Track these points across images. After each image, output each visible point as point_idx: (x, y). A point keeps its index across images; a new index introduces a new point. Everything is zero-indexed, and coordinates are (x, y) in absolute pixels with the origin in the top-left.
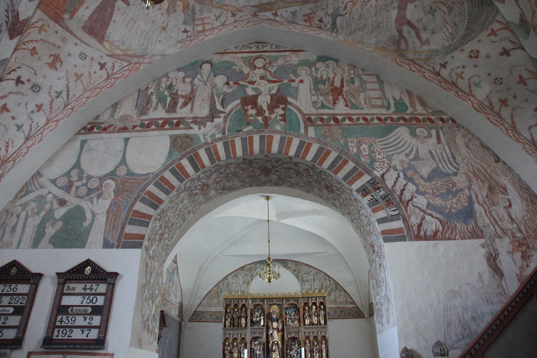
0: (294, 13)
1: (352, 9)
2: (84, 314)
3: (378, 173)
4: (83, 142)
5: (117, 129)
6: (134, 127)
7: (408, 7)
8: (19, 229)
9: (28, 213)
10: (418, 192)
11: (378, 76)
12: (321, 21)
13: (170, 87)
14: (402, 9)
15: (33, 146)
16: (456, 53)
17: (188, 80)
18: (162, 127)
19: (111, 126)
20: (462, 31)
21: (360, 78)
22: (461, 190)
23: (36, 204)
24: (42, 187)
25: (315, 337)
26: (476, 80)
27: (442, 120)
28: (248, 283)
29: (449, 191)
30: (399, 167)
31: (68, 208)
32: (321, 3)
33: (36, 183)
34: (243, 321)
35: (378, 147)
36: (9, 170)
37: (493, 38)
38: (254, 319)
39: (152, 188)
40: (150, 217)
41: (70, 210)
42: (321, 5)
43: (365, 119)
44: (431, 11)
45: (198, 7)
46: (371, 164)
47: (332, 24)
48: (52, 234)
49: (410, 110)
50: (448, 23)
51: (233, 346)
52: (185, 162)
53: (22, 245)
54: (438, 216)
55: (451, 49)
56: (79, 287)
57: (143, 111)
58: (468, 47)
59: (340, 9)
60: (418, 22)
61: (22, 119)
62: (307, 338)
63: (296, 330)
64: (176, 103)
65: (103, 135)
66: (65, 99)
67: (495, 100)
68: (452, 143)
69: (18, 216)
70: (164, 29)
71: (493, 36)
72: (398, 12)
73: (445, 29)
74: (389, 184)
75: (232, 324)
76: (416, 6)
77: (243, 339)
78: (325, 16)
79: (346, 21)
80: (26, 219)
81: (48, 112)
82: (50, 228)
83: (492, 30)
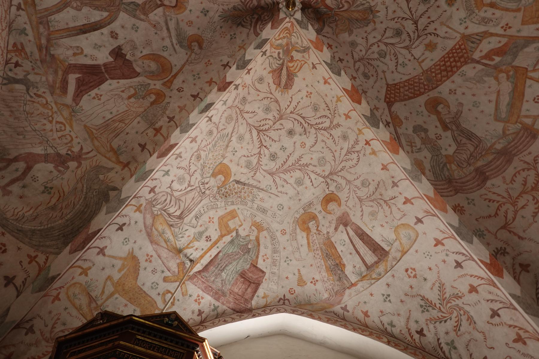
0: (23, 32)
1: (38, 103)
7: (49, 164)
12: (17, 65)
14: (45, 158)
20: (30, 227)
32: (41, 67)
37: (26, 260)
42: (38, 67)
44: (48, 189)
47: (13, 78)
50: (36, 210)
59: (35, 90)
60: (32, 177)
71: (29, 260)
72: (41, 154)
73: (28, 209)
76: (51, 172)
78: (25, 71)
79: (21, 96)
83: (36, 256)
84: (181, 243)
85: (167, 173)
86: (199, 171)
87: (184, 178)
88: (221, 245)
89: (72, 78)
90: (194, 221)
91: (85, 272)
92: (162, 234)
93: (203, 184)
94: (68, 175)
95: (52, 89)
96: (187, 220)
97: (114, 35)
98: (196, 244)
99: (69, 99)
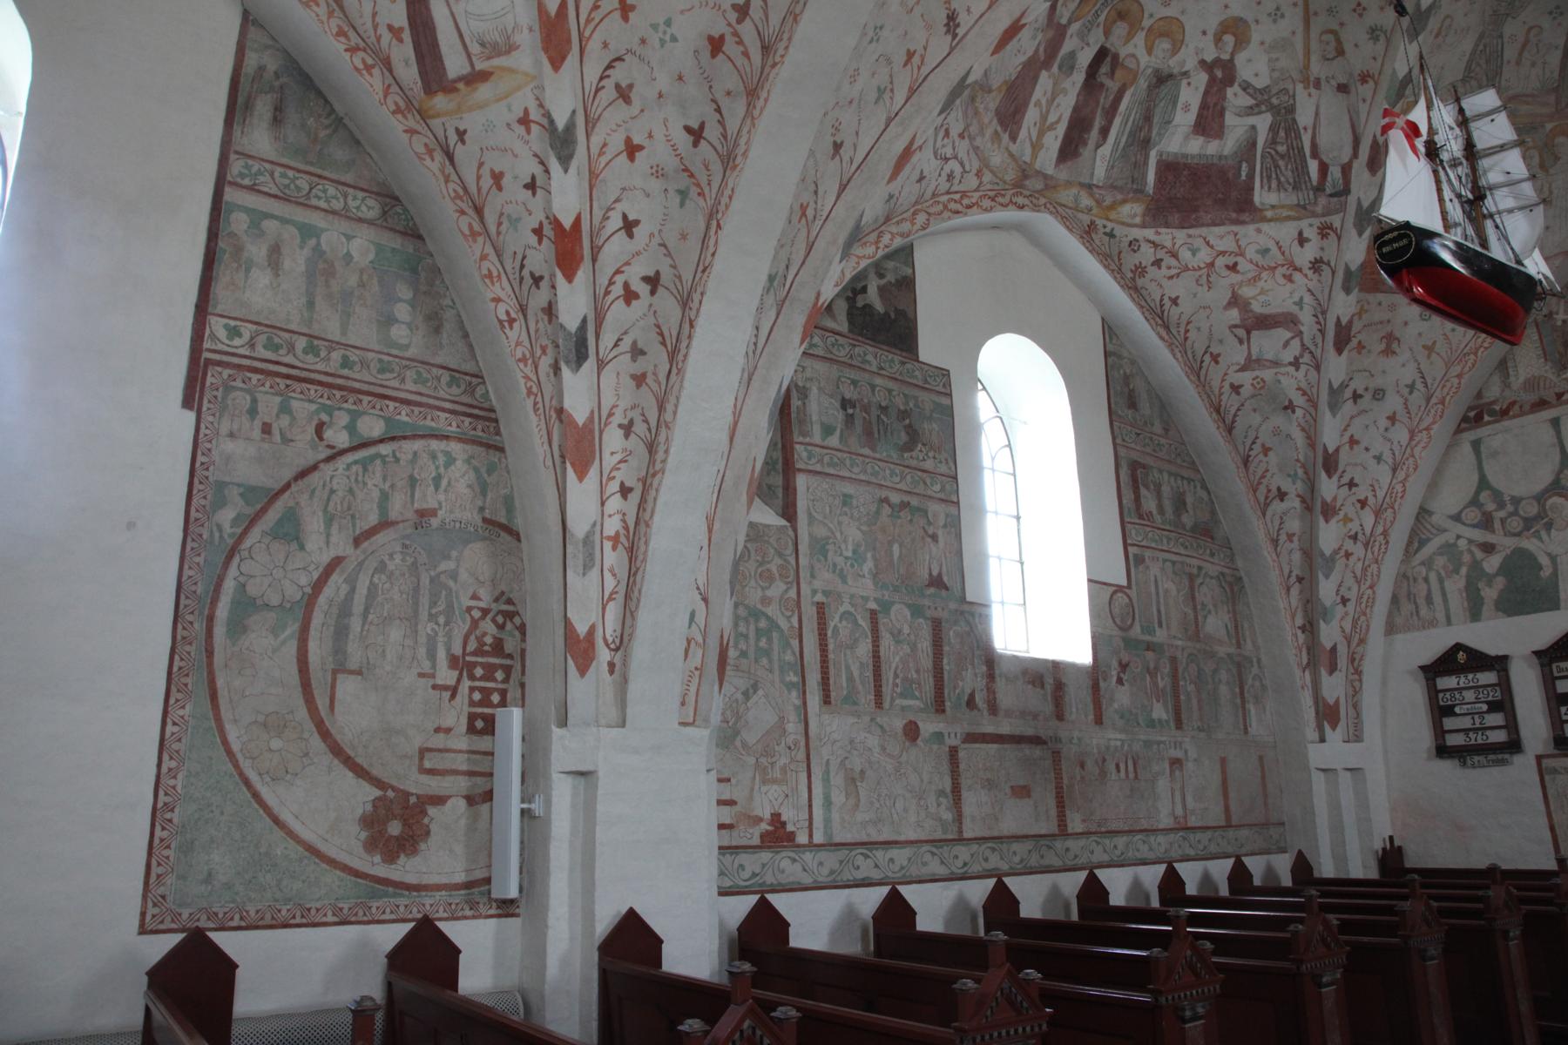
5: (1527, 407)
8: (1437, 598)
9: (1439, 574)
15: (1410, 479)
19: (1513, 403)
23: (1445, 558)
31: (1503, 554)
33: (1429, 527)
36: (1392, 523)
41: (1507, 558)
48: (1495, 597)
53: (1453, 619)
61: (1378, 446)
65: (1506, 423)
66: (1423, 389)
69: (1426, 580)
80: (1441, 581)
81: (1406, 420)
82: (1487, 589)
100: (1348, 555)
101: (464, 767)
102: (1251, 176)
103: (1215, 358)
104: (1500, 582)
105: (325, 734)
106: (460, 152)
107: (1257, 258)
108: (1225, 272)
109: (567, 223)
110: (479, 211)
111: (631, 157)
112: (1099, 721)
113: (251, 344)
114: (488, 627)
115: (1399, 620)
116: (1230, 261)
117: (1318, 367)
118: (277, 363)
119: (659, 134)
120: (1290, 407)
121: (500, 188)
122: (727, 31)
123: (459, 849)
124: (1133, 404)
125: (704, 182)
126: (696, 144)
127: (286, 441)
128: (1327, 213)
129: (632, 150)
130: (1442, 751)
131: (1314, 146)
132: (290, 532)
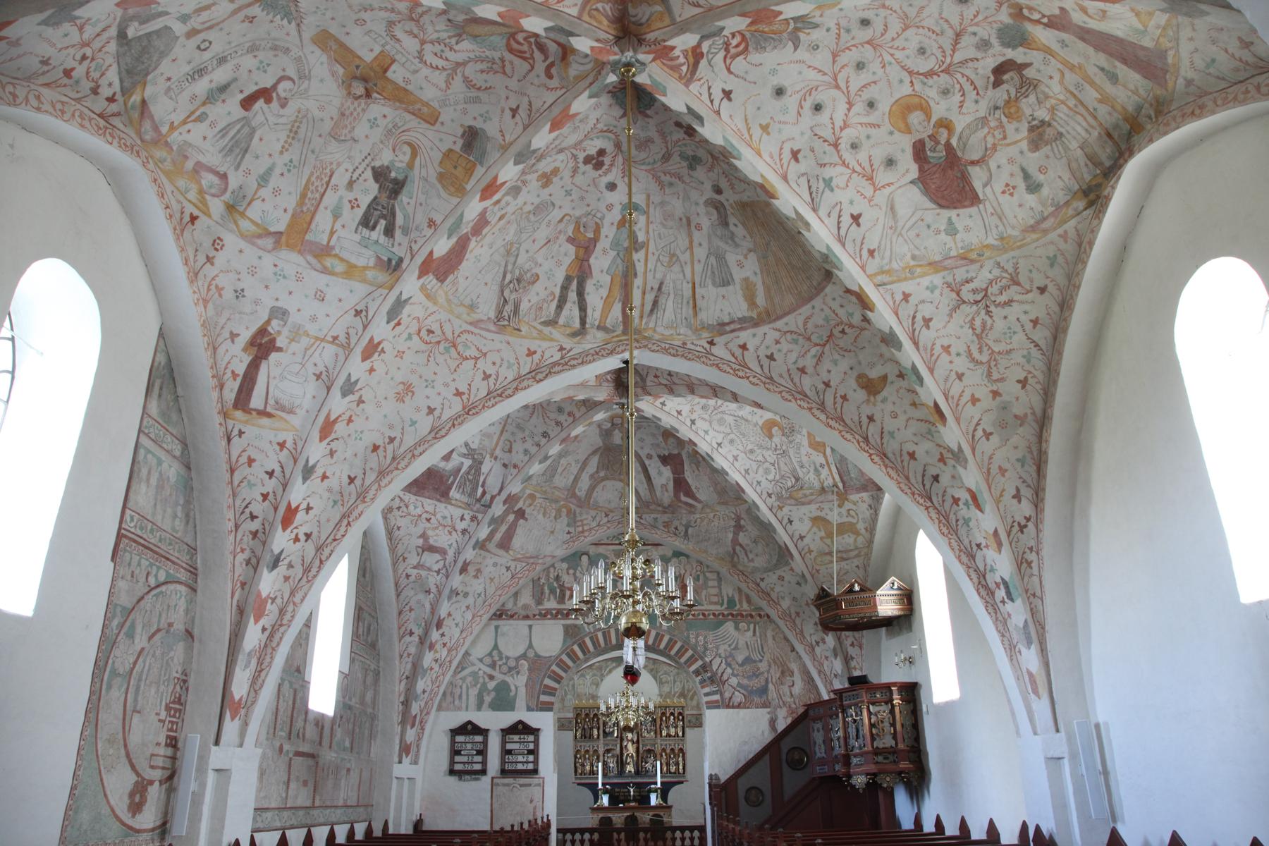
2: (523, 754)
3: (708, 660)
4: (497, 628)
6: (535, 615)
8: (464, 697)
10: (733, 674)
11: (718, 573)
12: (676, 529)
13: (557, 578)
16: (770, 574)
17: (571, 571)
18: (555, 617)
21: (705, 575)
22: (763, 673)
24: (473, 665)
25: (672, 750)
26: (782, 594)
27: (760, 616)
28: (597, 685)
29: (754, 674)
30: (723, 655)
34: (595, 732)
35: (710, 638)
38: (607, 730)
39: (554, 667)
40: (556, 689)
41: (498, 684)
43: (704, 615)
45: (578, 510)
46: (704, 652)
49: (738, 606)
51: (585, 759)
52: (576, 648)
54: (742, 691)
55: (767, 570)
56: (516, 738)
57: (539, 602)
58: (779, 572)
62: (664, 750)
63: (652, 742)
64: (564, 595)
65: (511, 622)
67: (793, 611)
68: (764, 636)
69: (461, 687)
70: (552, 532)
74: (715, 668)
75: (584, 736)
77: (596, 751)
84: (817, 485)
85: (759, 483)
86: (764, 452)
87: (767, 469)
88: (831, 460)
89: (684, 498)
90: (804, 470)
91: (810, 551)
92: (805, 496)
93: (776, 450)
94: (749, 528)
95: (691, 512)
96: (801, 475)
97: (649, 457)
98: (823, 477)
99: (699, 506)
100: (432, 669)
101: (161, 764)
102: (453, 483)
103: (404, 559)
104: (493, 694)
105: (126, 746)
106: (235, 440)
107: (440, 519)
108: (424, 521)
109: (293, 506)
110: (232, 471)
111: (322, 480)
112: (330, 747)
113: (135, 526)
114: (178, 688)
115: (444, 705)
116: (428, 516)
117: (447, 577)
118: (141, 537)
119: (338, 474)
120: (428, 592)
121: (250, 466)
122: (382, 445)
123: (153, 810)
124: (364, 576)
125: (346, 500)
126: (350, 484)
127: (138, 581)
128: (478, 511)
129: (324, 477)
130: (452, 772)
131: (484, 482)
132: (131, 636)
